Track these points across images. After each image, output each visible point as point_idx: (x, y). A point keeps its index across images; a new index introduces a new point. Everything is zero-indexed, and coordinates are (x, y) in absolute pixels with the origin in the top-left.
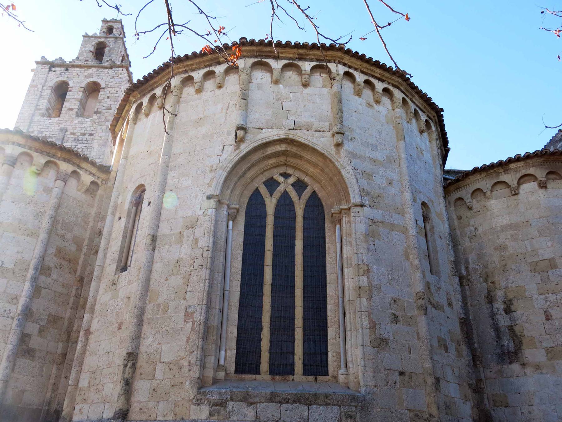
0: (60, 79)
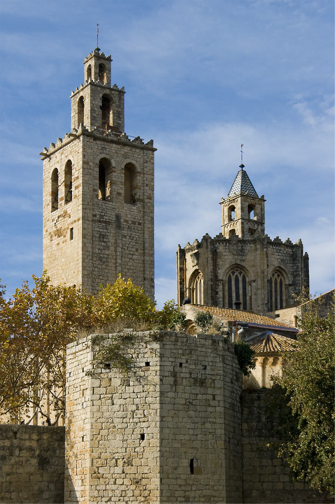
0: (103, 156)
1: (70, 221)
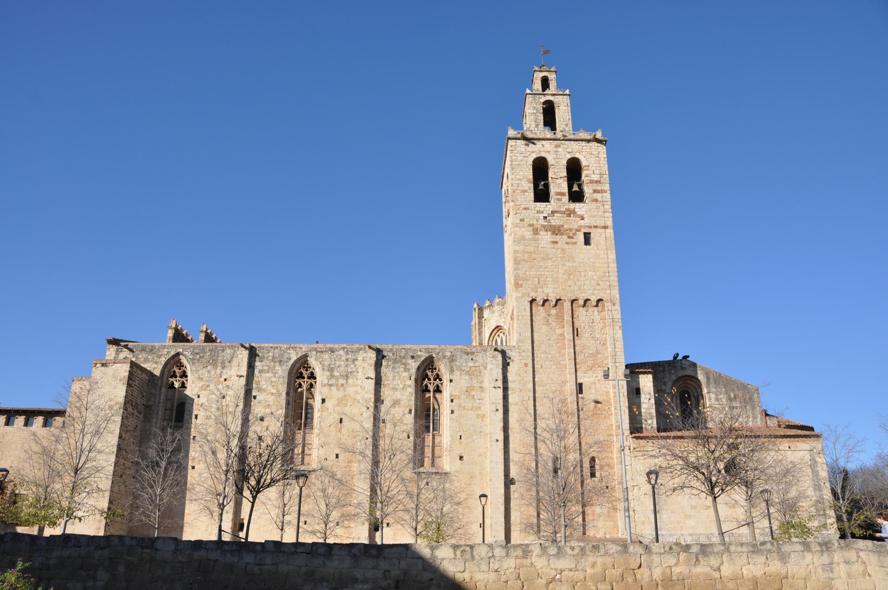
1: (582, 223)
